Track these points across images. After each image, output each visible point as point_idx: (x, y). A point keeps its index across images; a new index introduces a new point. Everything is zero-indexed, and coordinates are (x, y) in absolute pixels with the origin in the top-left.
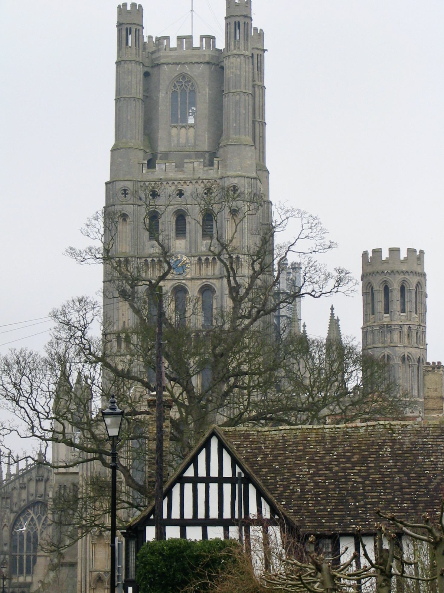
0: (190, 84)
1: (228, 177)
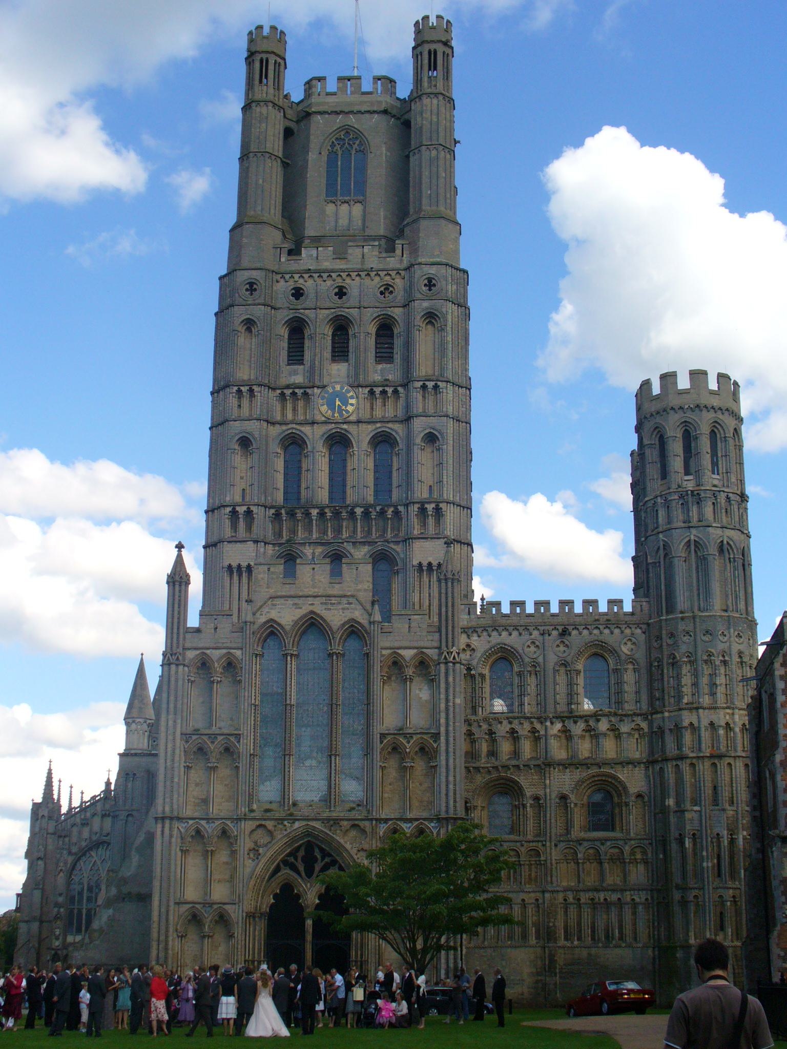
0: (357, 142)
1: (420, 264)
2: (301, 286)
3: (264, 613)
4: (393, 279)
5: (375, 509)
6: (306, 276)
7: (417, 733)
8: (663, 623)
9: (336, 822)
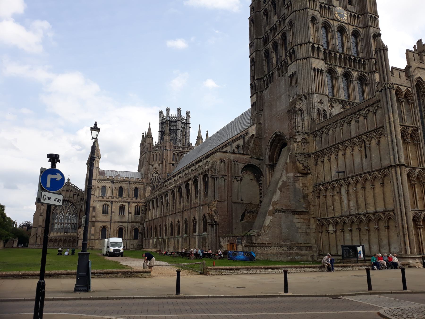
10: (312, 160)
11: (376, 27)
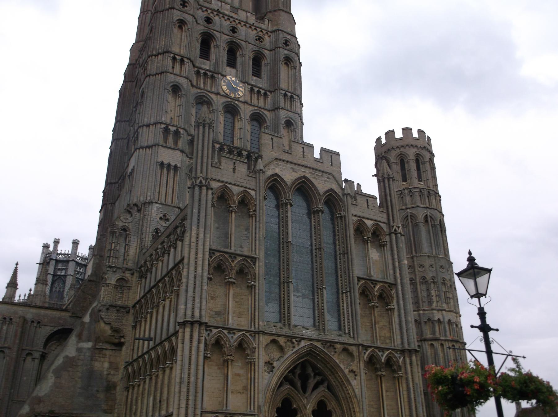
2: (212, 18)
3: (271, 168)
4: (264, 35)
5: (255, 155)
6: (215, 13)
7: (381, 282)
8: (415, 259)
9: (331, 344)
10: (130, 319)
11: (292, 111)
